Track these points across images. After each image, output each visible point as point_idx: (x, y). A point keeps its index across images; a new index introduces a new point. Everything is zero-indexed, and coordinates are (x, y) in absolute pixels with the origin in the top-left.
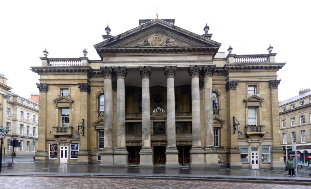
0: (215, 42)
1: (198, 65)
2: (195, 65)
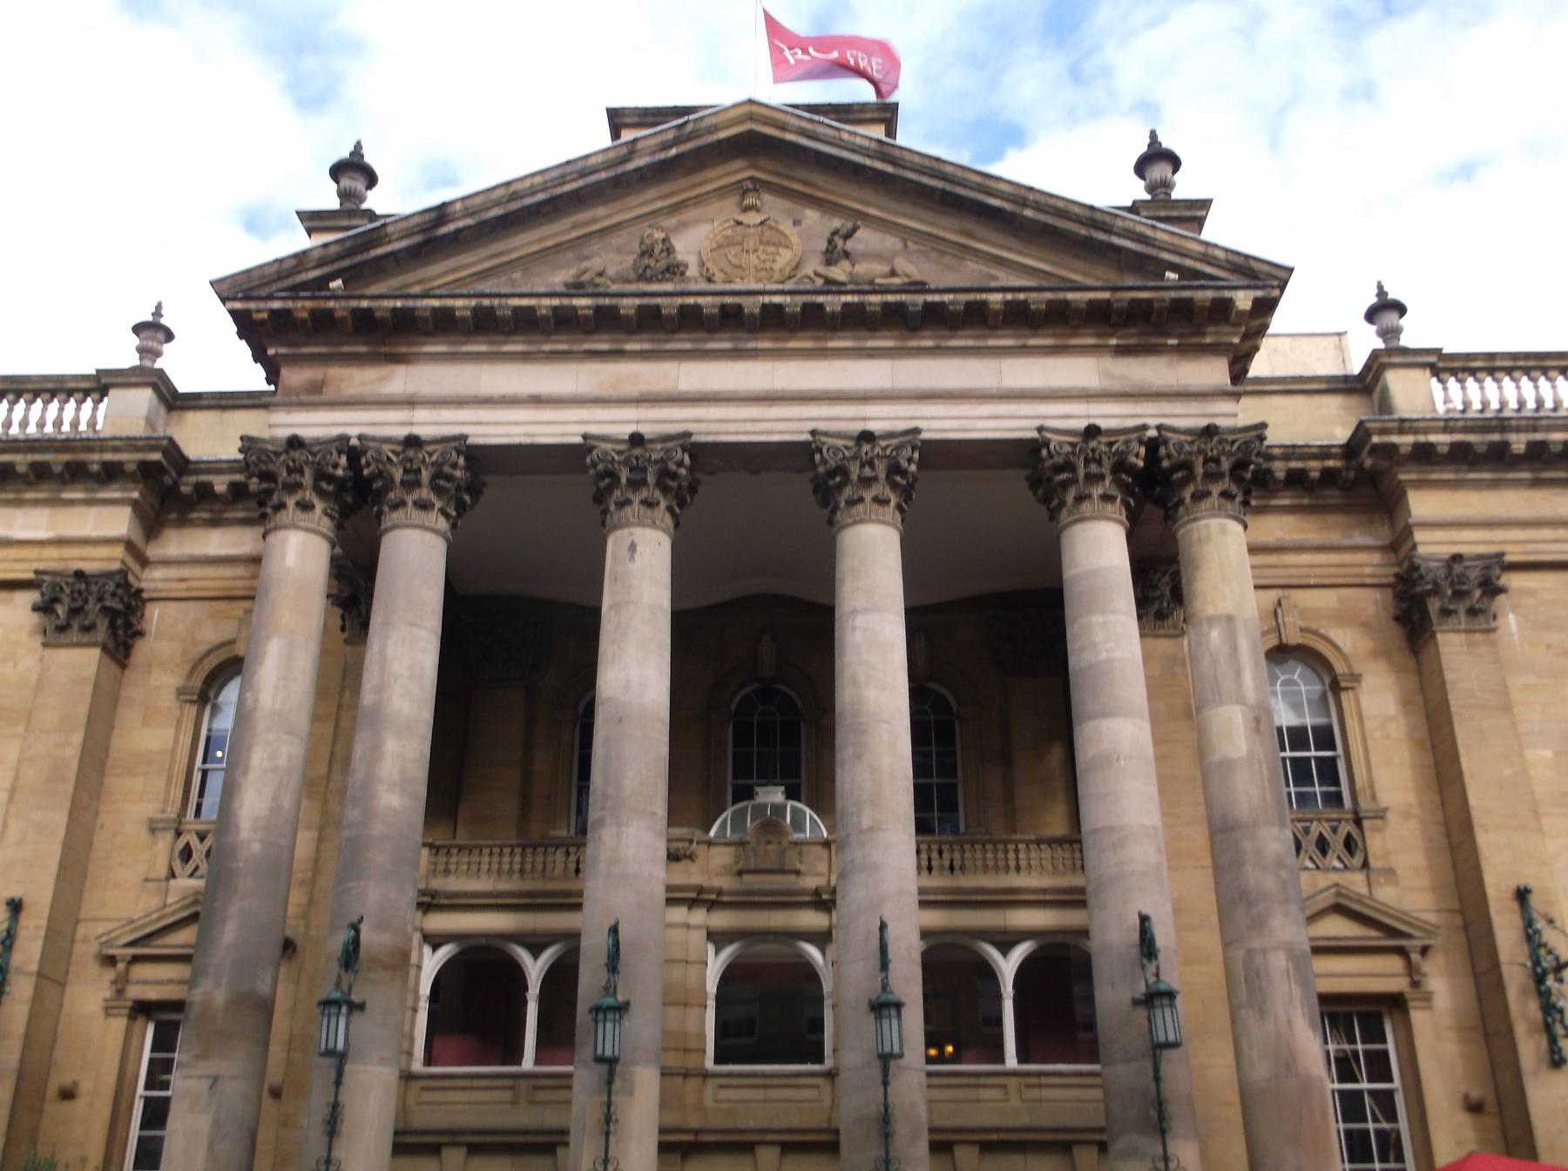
0: (1231, 257)
1: (1104, 424)
2: (1082, 424)
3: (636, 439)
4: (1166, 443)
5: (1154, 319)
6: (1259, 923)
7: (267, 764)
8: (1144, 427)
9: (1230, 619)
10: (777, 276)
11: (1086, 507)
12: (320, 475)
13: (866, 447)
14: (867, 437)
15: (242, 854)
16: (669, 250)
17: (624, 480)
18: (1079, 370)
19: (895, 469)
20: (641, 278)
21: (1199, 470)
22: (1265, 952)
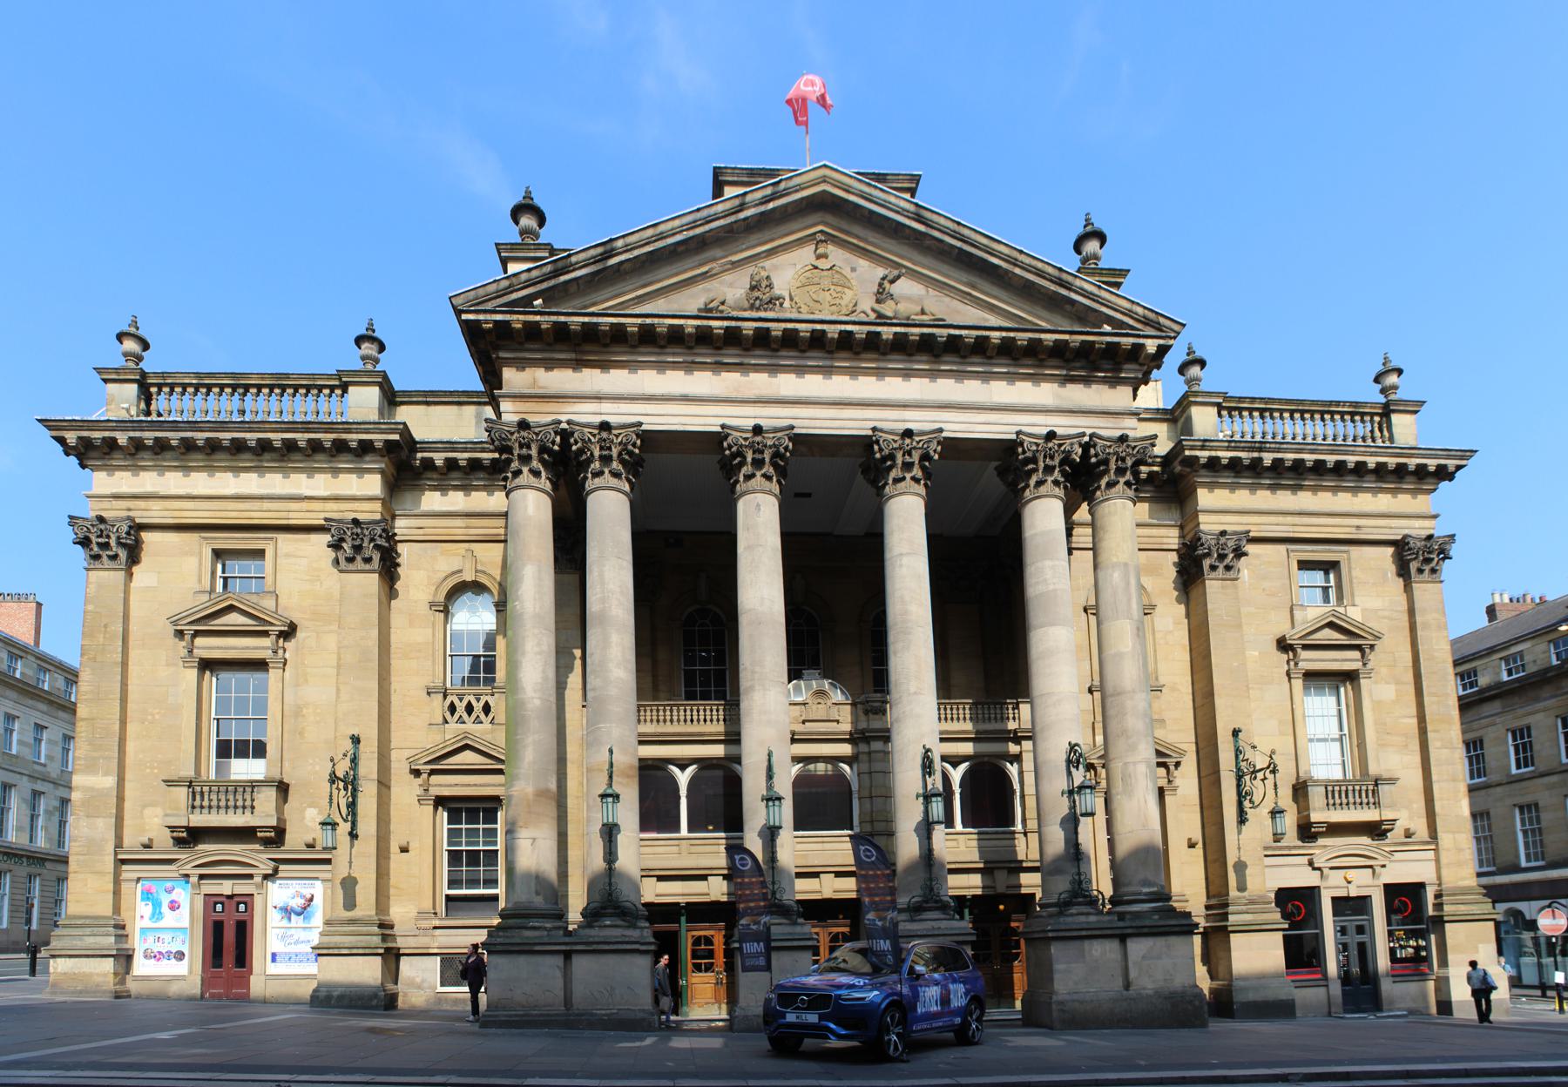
3: (757, 430)
4: (1094, 446)
5: (1092, 358)
6: (1133, 748)
7: (536, 649)
8: (1084, 434)
9: (1126, 565)
10: (844, 311)
11: (1043, 490)
12: (543, 449)
13: (908, 441)
14: (908, 433)
15: (530, 706)
16: (770, 286)
17: (749, 459)
18: (1045, 393)
19: (925, 457)
20: (752, 307)
21: (1113, 466)
22: (1135, 763)
